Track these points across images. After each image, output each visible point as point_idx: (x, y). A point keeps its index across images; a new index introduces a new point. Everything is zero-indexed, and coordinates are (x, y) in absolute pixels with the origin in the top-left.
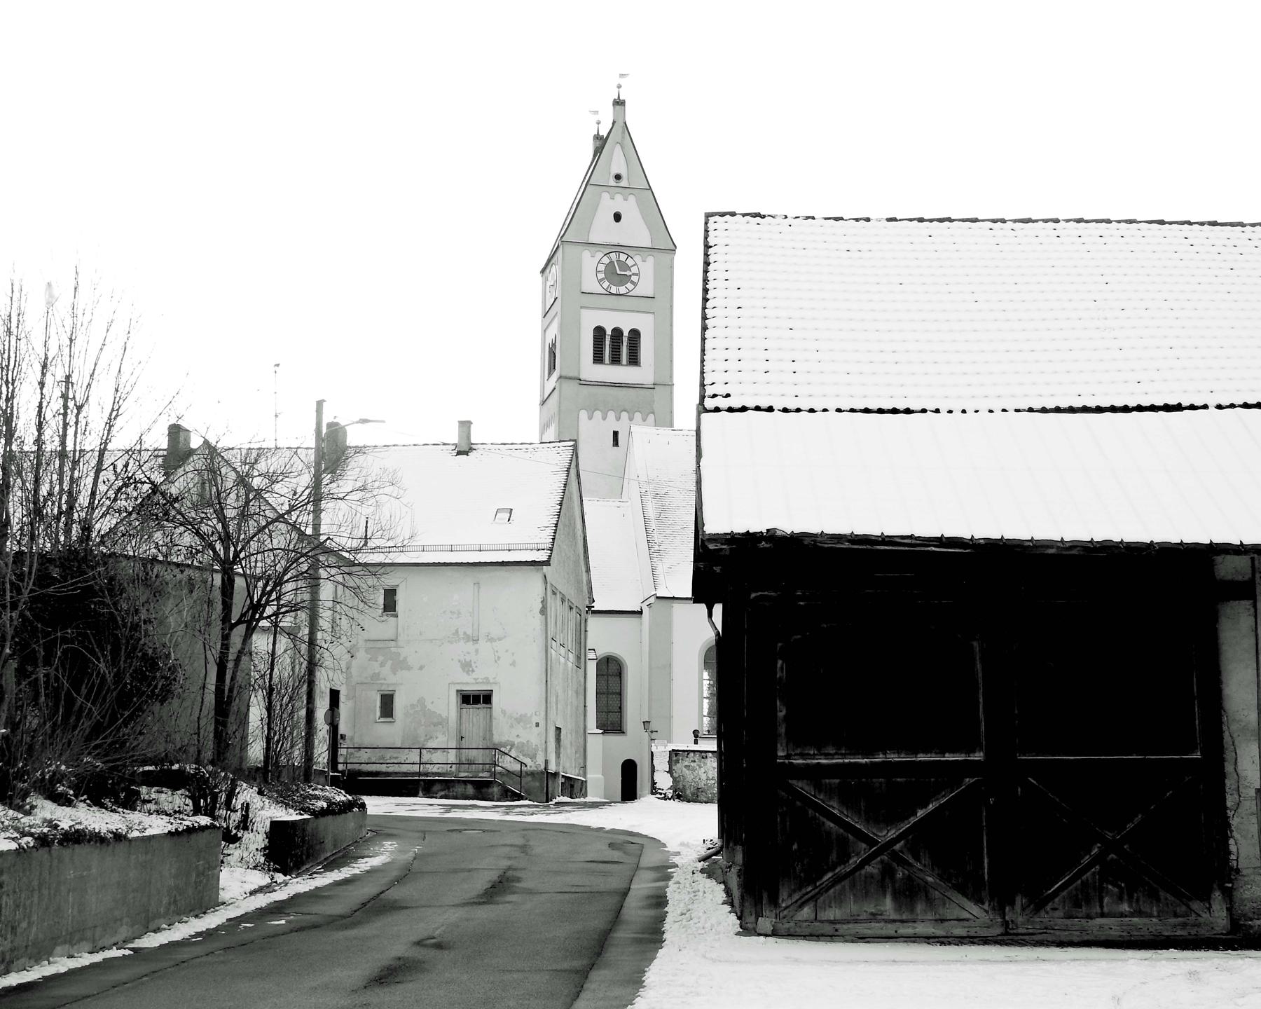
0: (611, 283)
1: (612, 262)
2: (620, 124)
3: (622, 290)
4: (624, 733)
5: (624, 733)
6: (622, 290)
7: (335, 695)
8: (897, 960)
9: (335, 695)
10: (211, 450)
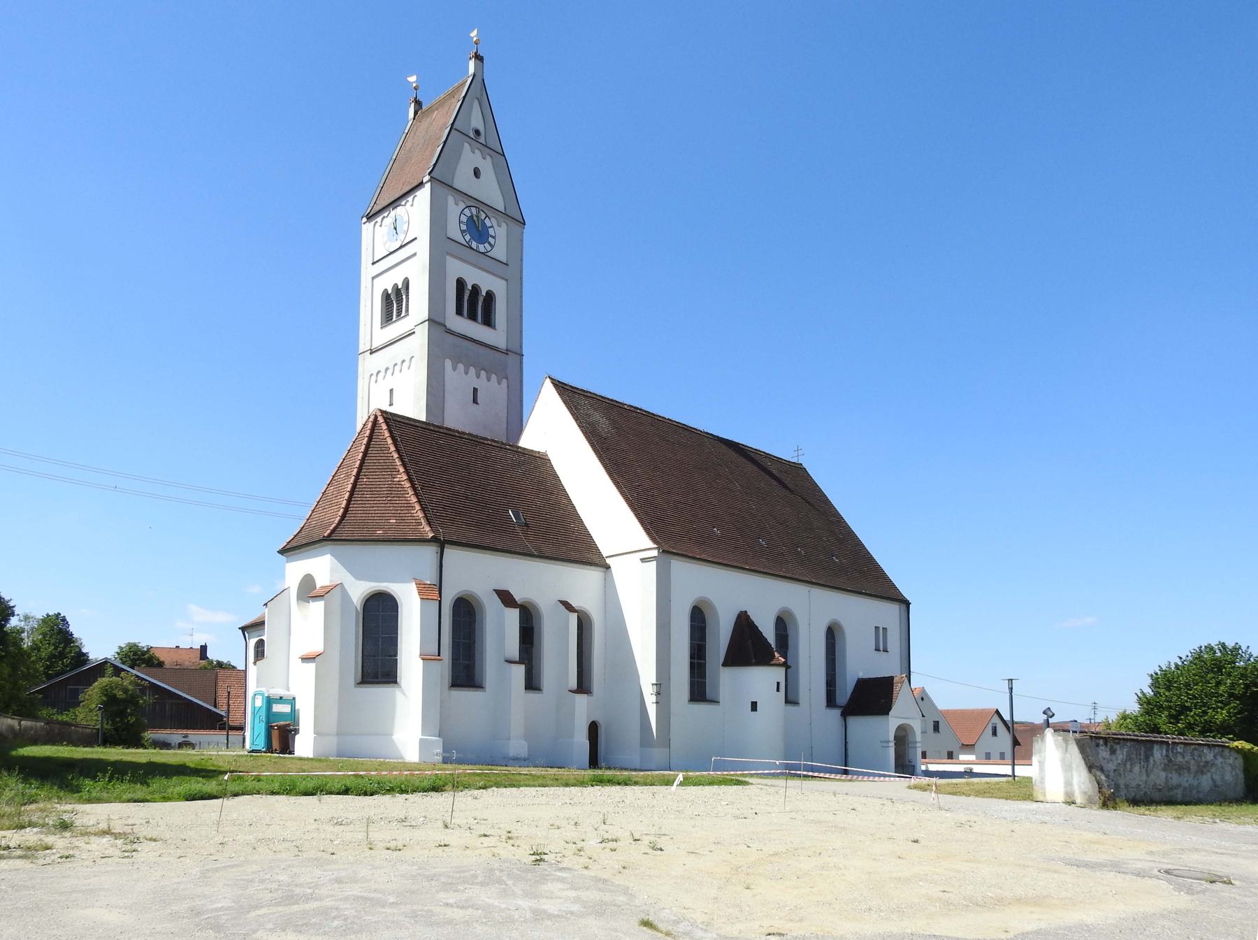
0: (472, 238)
1: (472, 216)
2: (478, 79)
3: (481, 248)
4: (483, 688)
5: (483, 688)
6: (481, 248)
7: (778, 690)
8: (487, 834)
9: (778, 690)
10: (1065, 787)
